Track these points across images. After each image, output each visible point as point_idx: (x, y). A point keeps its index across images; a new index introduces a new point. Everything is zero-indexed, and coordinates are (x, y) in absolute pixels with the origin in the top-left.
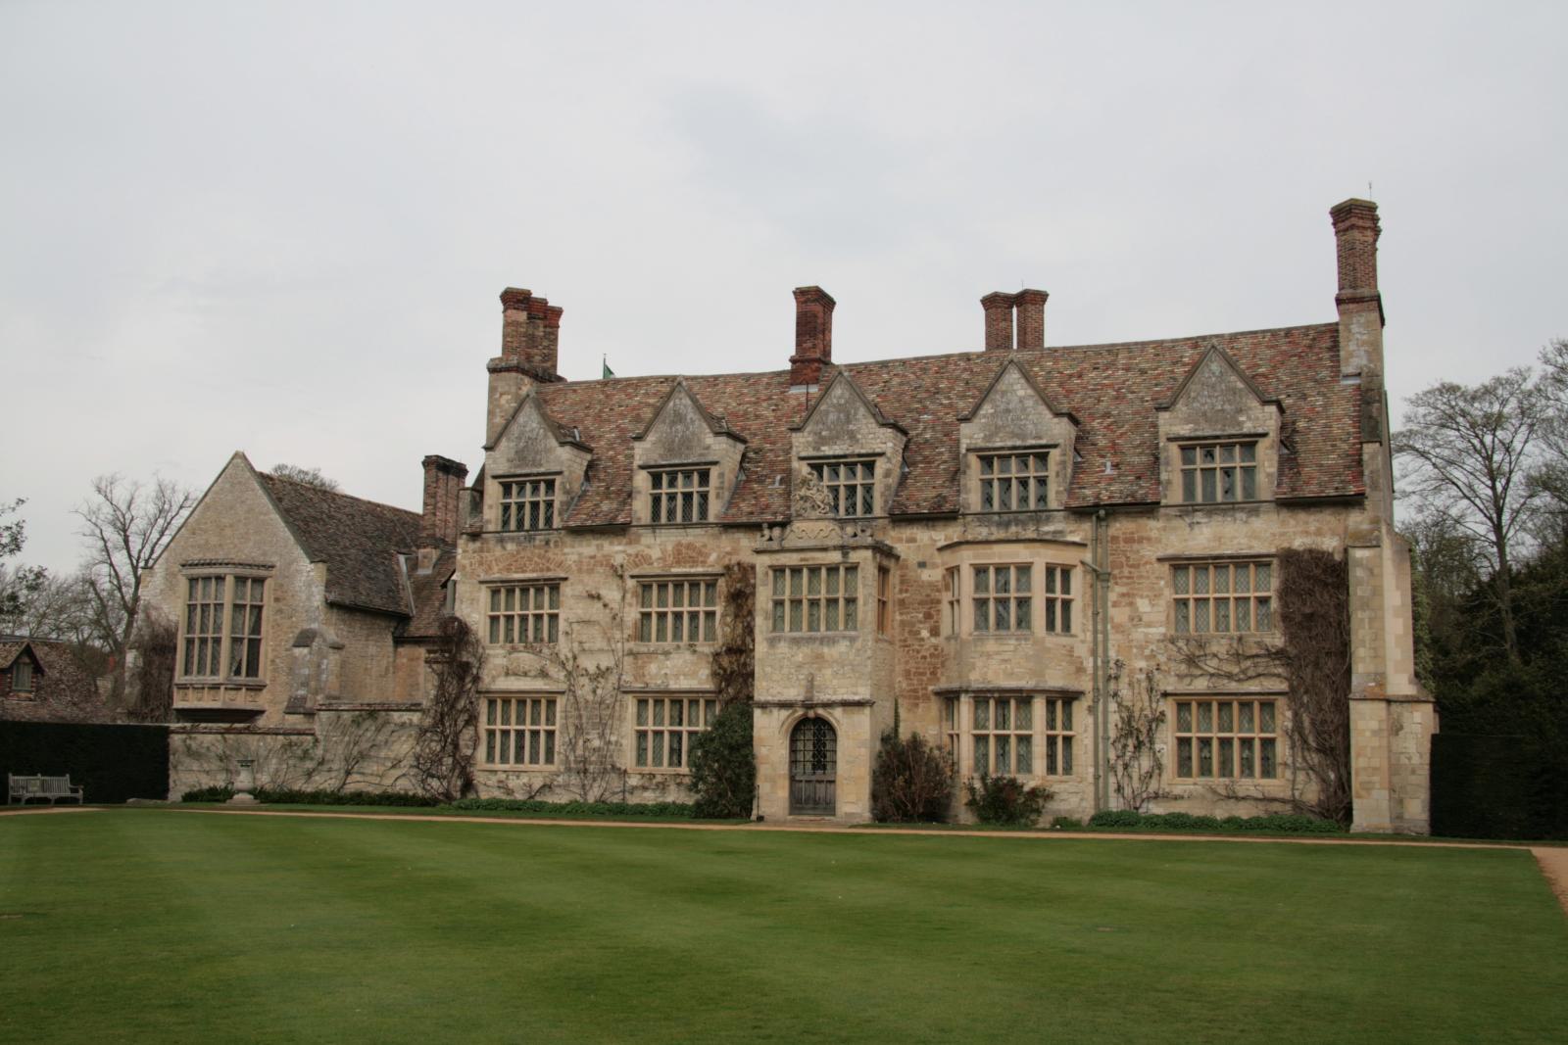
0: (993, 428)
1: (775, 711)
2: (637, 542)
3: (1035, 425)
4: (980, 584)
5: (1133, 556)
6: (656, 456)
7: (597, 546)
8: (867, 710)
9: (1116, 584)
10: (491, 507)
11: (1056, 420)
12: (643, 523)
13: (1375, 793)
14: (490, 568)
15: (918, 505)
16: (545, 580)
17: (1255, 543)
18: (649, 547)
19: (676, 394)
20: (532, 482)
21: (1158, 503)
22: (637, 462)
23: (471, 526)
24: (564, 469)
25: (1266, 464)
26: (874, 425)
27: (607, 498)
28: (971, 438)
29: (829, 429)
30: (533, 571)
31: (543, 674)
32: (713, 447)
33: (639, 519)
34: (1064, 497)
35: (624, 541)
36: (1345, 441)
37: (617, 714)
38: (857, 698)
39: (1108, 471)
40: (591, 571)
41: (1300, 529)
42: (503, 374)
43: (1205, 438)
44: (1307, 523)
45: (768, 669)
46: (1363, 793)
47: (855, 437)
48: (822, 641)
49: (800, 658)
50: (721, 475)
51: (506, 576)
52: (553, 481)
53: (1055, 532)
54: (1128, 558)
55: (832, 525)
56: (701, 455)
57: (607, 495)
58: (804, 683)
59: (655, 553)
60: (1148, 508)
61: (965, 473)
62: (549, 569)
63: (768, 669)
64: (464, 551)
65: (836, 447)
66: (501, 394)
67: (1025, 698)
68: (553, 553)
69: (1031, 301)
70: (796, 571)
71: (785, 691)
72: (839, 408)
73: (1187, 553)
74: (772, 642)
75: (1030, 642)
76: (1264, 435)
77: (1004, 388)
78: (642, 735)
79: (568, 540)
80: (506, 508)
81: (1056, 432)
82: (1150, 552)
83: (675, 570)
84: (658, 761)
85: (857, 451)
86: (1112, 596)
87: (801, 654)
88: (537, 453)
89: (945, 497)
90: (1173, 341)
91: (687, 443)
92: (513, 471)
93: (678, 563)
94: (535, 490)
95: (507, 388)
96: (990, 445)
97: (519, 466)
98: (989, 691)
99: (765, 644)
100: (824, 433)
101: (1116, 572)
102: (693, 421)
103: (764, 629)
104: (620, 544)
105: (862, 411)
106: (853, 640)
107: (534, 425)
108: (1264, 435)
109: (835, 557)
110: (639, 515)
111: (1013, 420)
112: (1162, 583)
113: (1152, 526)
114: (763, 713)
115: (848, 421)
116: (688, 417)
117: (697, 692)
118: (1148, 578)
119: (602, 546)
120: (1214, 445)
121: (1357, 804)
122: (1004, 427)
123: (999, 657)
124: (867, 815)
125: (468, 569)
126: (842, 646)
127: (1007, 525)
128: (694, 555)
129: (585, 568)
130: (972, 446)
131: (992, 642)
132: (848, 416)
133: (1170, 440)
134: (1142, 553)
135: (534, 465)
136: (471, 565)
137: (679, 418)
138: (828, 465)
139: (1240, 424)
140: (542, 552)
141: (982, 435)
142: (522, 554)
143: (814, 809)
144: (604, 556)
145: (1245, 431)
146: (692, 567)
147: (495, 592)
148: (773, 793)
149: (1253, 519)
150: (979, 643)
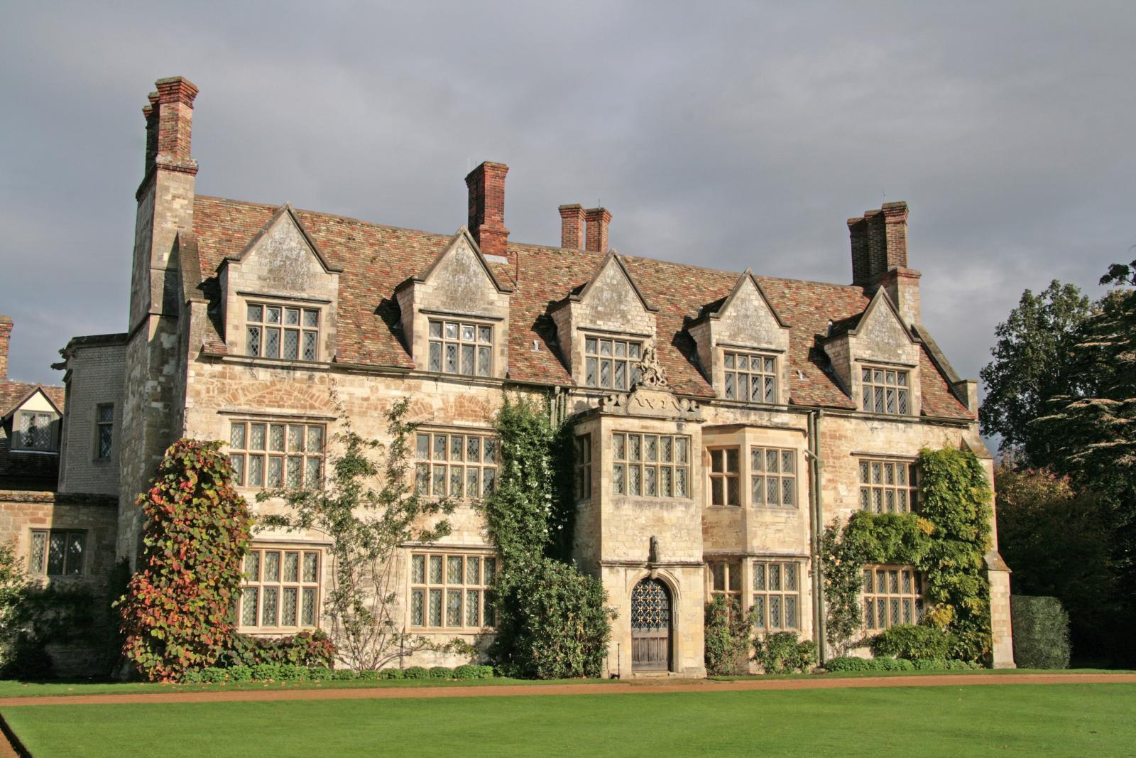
0: (736, 329)
1: (622, 570)
2: (418, 388)
3: (767, 332)
4: (757, 465)
5: (836, 450)
6: (438, 303)
7: (371, 388)
8: (701, 571)
9: (825, 471)
10: (236, 327)
11: (781, 330)
12: (424, 370)
13: (1004, 638)
14: (235, 397)
15: (681, 387)
16: (309, 418)
17: (910, 448)
18: (429, 396)
19: (458, 242)
20: (289, 307)
21: (854, 409)
22: (416, 307)
23: (211, 345)
24: (331, 299)
25: (915, 389)
26: (642, 309)
27: (367, 338)
28: (720, 334)
29: (603, 305)
30: (292, 407)
31: (305, 523)
32: (499, 304)
33: (421, 365)
34: (788, 395)
35: (403, 386)
36: (935, 378)
37: (393, 570)
38: (692, 560)
39: (801, 376)
40: (363, 414)
41: (934, 440)
42: (176, 173)
43: (880, 363)
44: (939, 436)
45: (614, 530)
46: (998, 639)
47: (626, 317)
48: (661, 505)
49: (642, 520)
50: (504, 333)
51: (256, 408)
52: (317, 311)
53: (782, 424)
54: (832, 451)
55: (670, 399)
56: (485, 309)
57: (364, 336)
58: (648, 545)
59: (437, 403)
60: (845, 412)
61: (716, 364)
62: (312, 407)
63: (614, 530)
64: (198, 375)
65: (610, 323)
66: (174, 197)
67: (792, 563)
68: (319, 389)
69: (596, 216)
70: (636, 436)
71: (631, 552)
72: (613, 288)
73: (871, 451)
74: (617, 504)
75: (796, 516)
76: (913, 366)
77: (743, 296)
78: (419, 594)
79: (337, 376)
80: (254, 332)
81: (782, 340)
82: (846, 448)
83: (457, 423)
84: (439, 622)
85: (628, 331)
86: (823, 481)
87: (645, 516)
88: (297, 275)
89: (695, 383)
90: (770, 279)
91: (471, 295)
92: (265, 291)
93: (461, 415)
94: (295, 319)
95: (181, 191)
96: (734, 343)
97: (274, 287)
98: (771, 556)
99: (610, 503)
100: (599, 308)
101: (826, 461)
102: (475, 274)
103: (611, 490)
104: (397, 389)
105: (632, 294)
106: (688, 506)
107: (294, 244)
108: (913, 366)
109: (670, 427)
110: (419, 361)
111: (750, 325)
112: (855, 473)
113: (848, 426)
114: (611, 572)
115: (620, 302)
116: (471, 269)
117: (483, 549)
118: (846, 468)
119: (377, 388)
120: (882, 370)
121: (995, 647)
122: (745, 329)
123: (775, 527)
124: (703, 672)
125: (204, 395)
126: (679, 512)
127: (748, 415)
128: (477, 409)
129: (356, 410)
130: (721, 342)
131: (769, 513)
132: (620, 296)
133: (856, 360)
134: (842, 448)
135: (293, 288)
136: (208, 392)
137: (461, 267)
138: (603, 339)
139: (899, 355)
140: (305, 386)
141: (728, 333)
142: (278, 387)
143: (649, 665)
144: (379, 399)
145: (902, 361)
146: (473, 421)
147: (235, 424)
148: (619, 654)
149: (908, 429)
150: (759, 514)
